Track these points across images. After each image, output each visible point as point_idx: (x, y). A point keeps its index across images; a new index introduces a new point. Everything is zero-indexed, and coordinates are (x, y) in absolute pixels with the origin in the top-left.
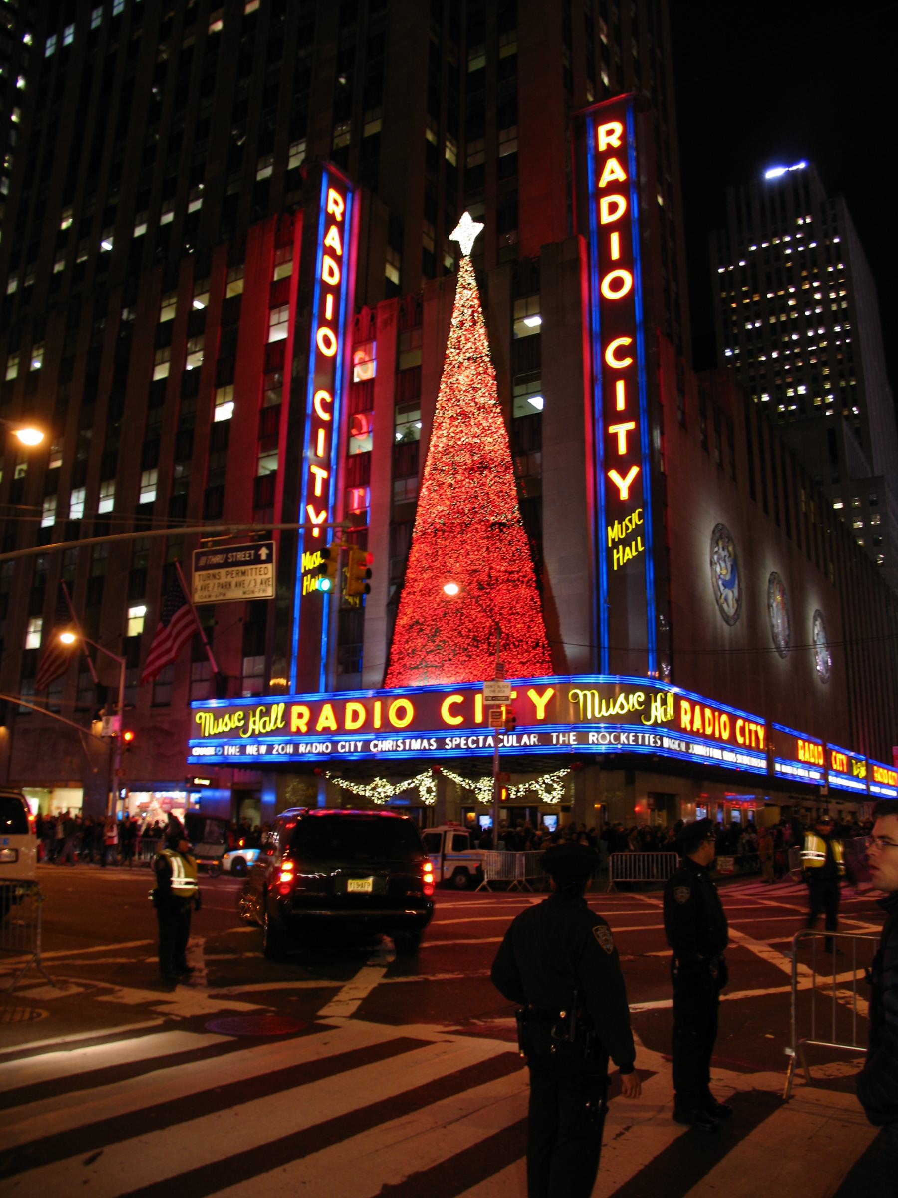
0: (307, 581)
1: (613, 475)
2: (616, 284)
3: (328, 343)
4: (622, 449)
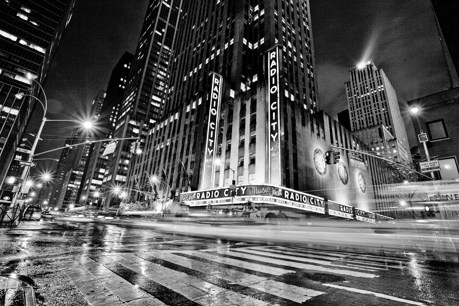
1: (272, 135)
2: (274, 90)
3: (214, 112)
4: (274, 129)
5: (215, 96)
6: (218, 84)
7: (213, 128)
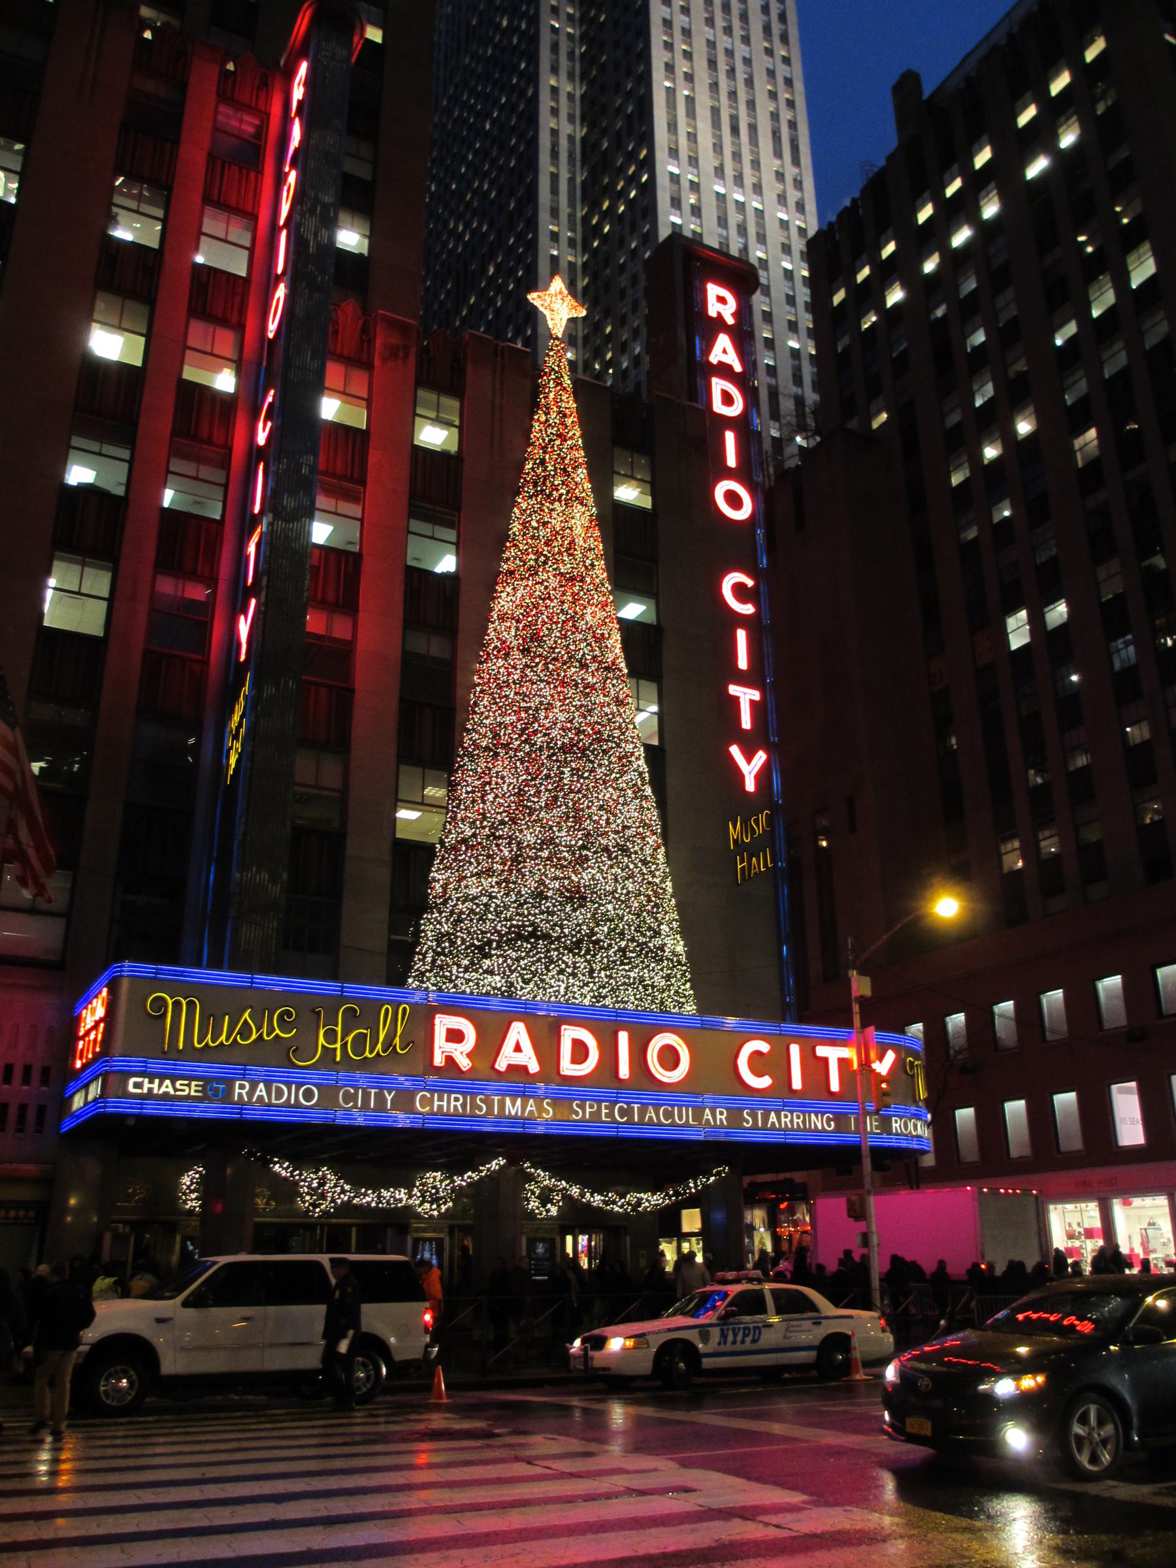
0: (742, 861)
3: (734, 500)
5: (727, 399)
6: (730, 321)
7: (748, 609)
